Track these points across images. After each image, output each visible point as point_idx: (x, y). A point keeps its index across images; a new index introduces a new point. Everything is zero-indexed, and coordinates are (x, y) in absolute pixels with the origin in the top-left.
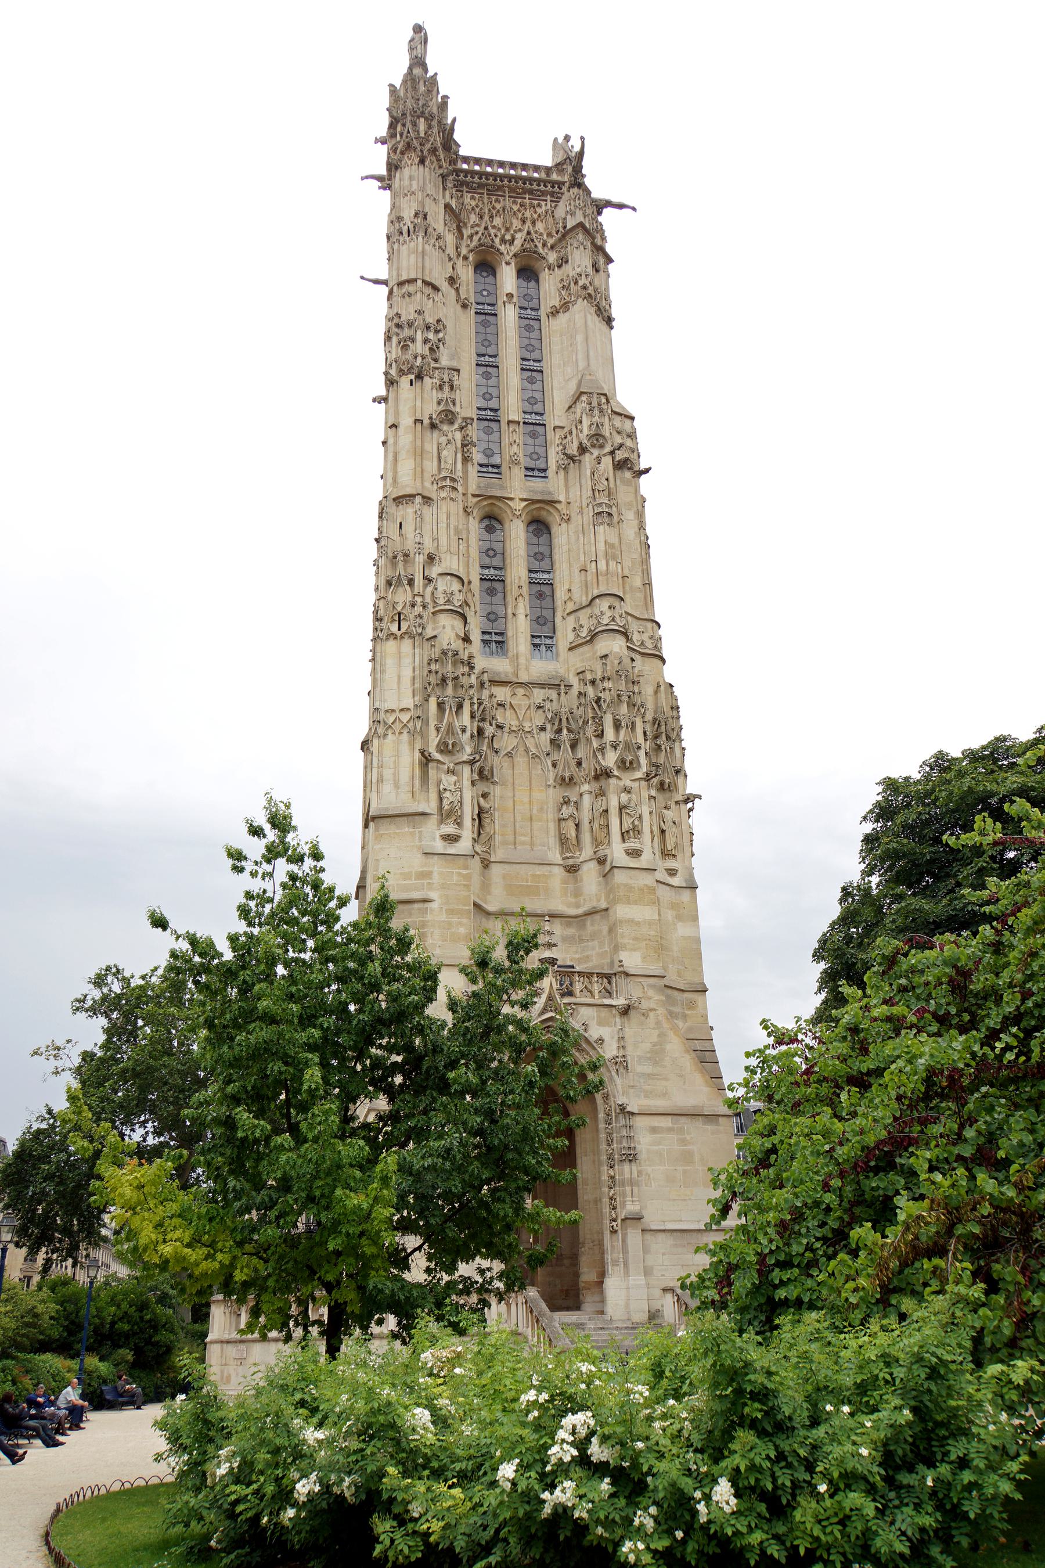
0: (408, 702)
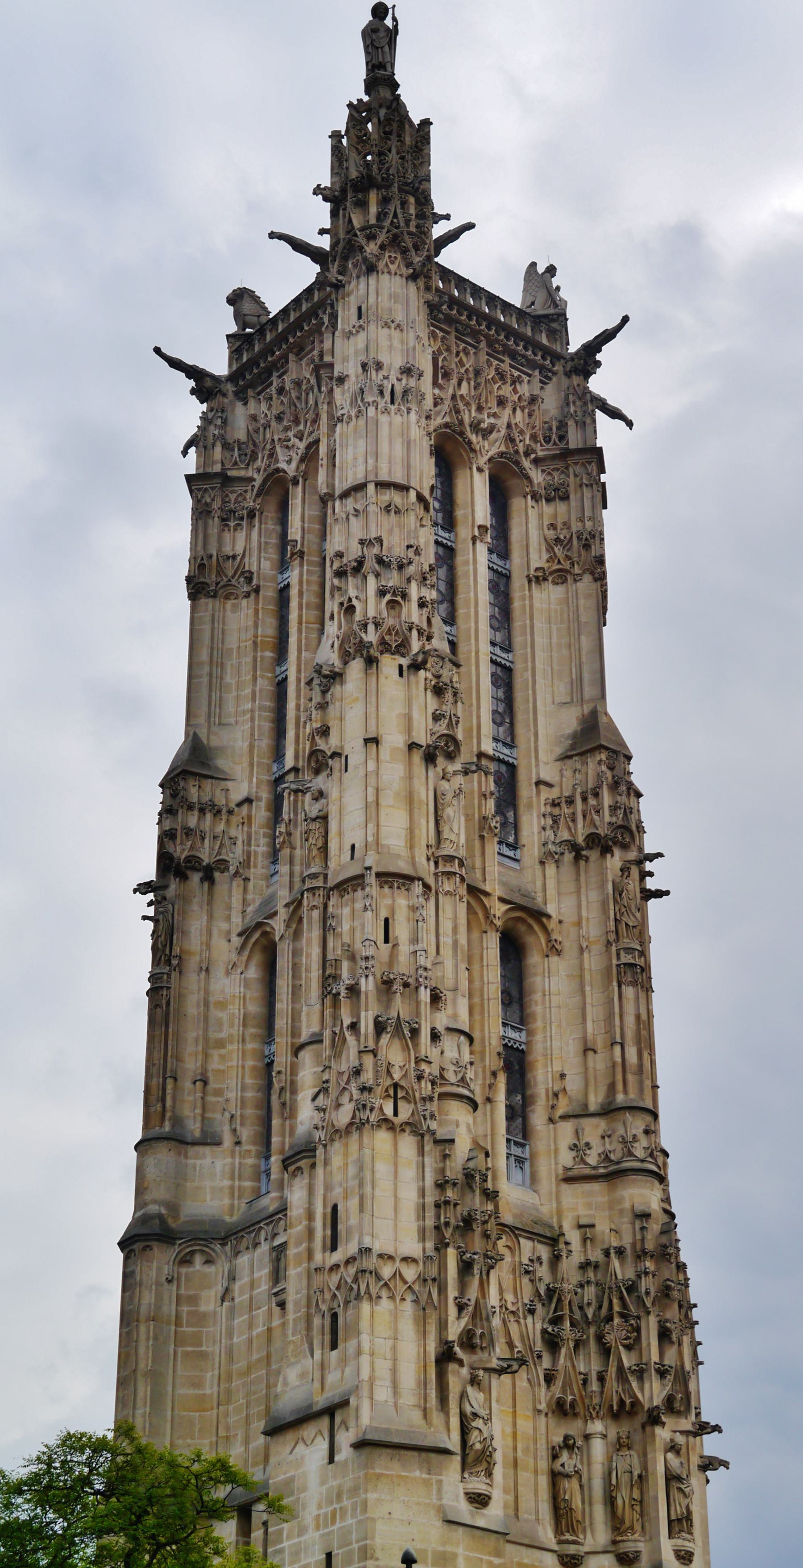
0: (411, 1246)
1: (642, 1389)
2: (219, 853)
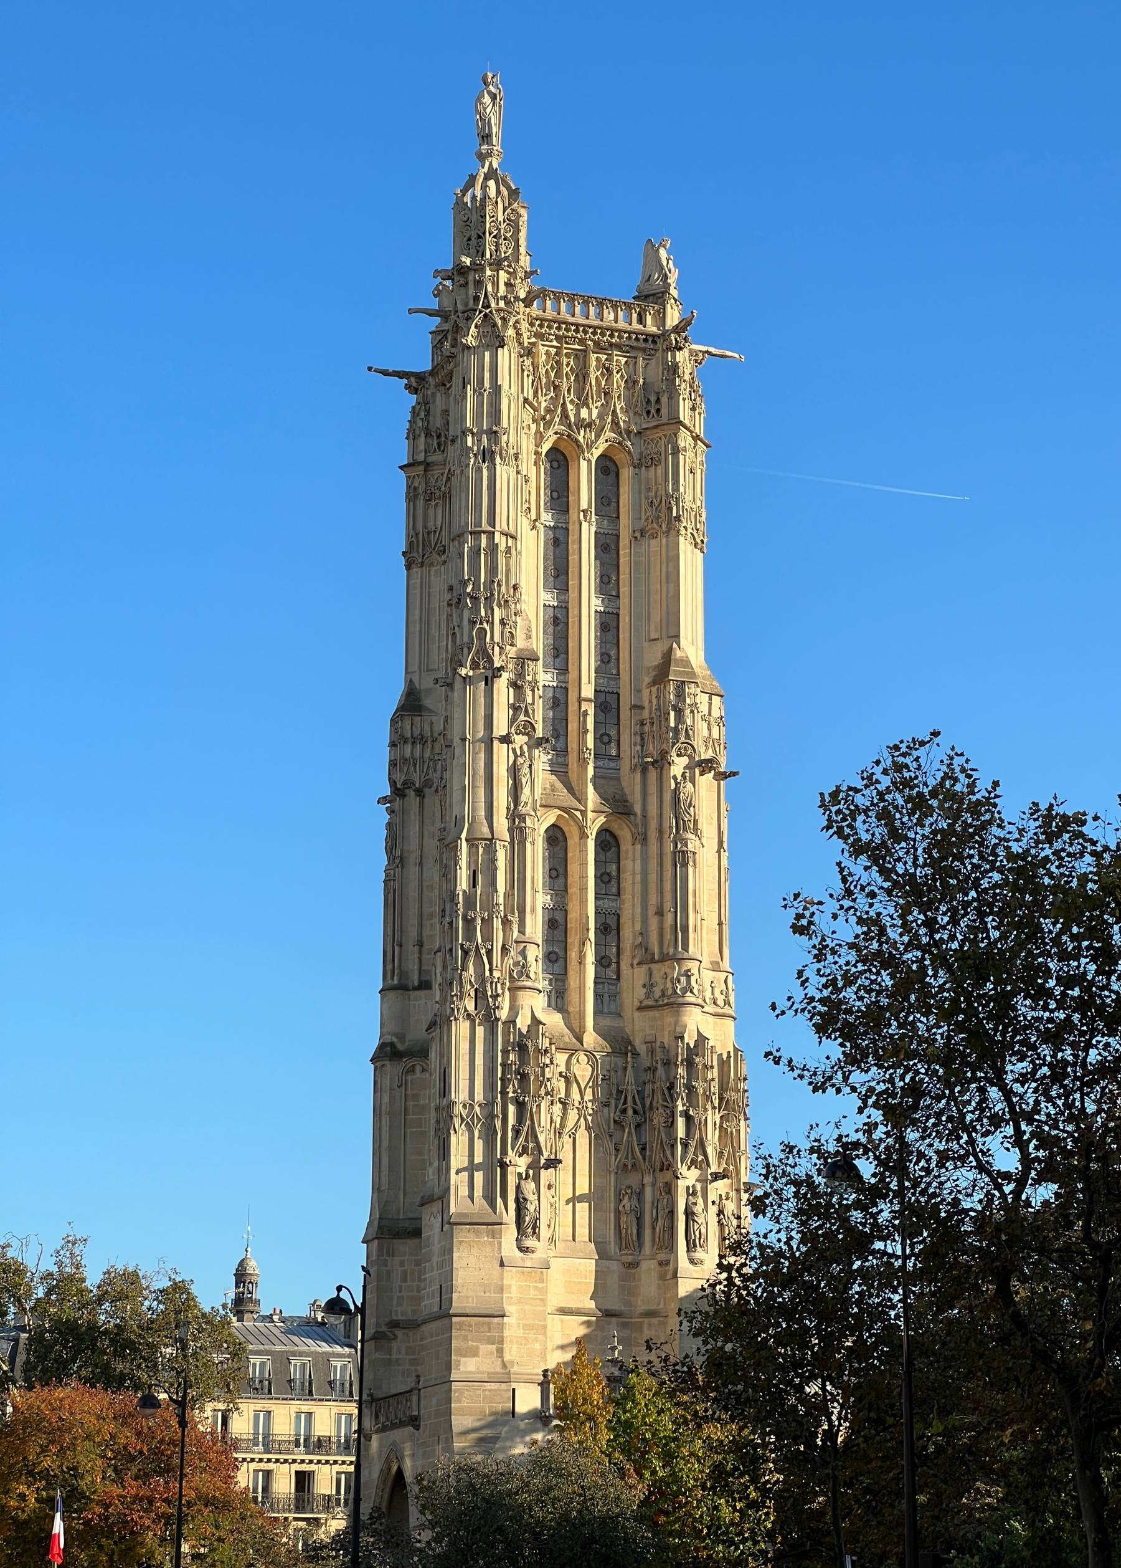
1: (673, 1154)
2: (427, 774)
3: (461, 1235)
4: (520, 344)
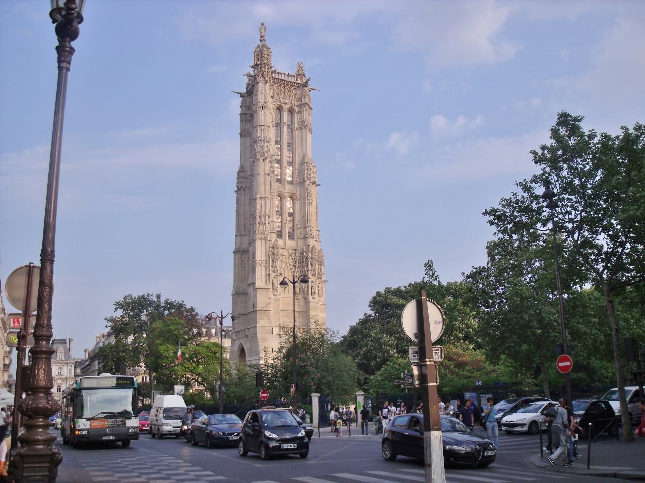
3: (259, 292)
4: (270, 82)
